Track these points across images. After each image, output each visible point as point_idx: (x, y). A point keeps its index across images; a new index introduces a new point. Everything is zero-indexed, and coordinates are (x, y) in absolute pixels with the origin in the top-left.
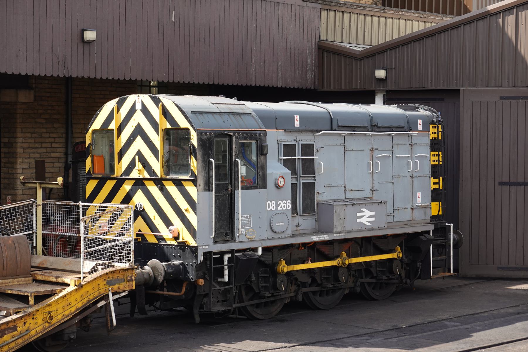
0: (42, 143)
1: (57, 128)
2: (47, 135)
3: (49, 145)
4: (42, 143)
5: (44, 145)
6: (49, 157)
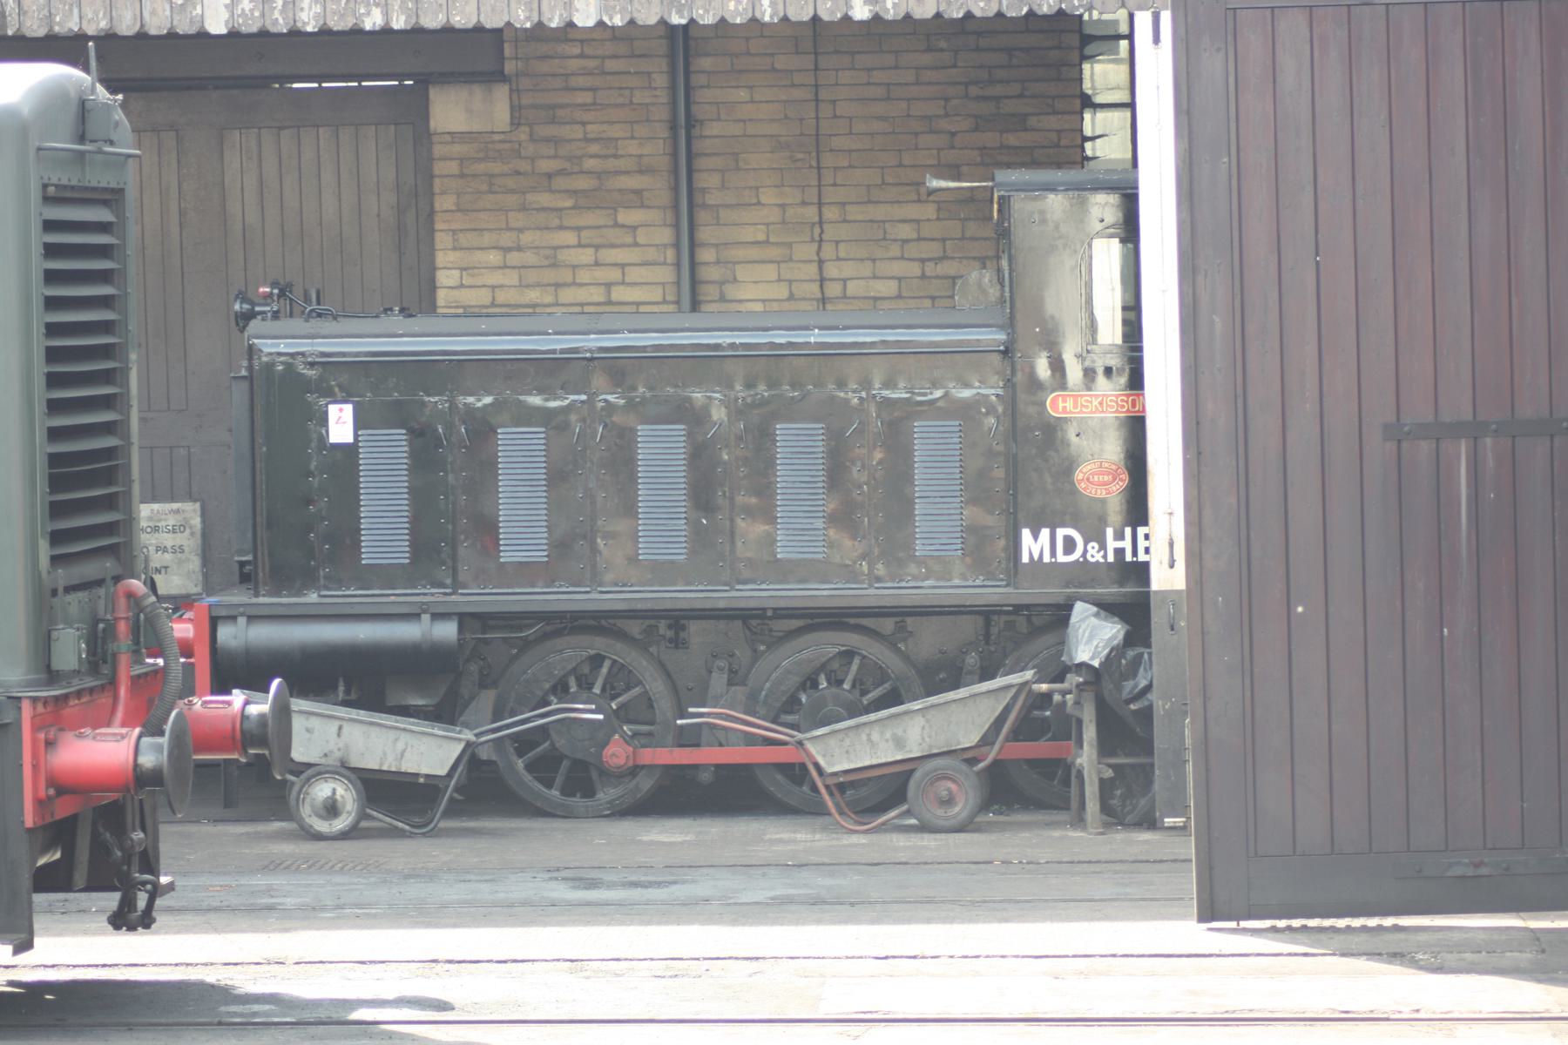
0: (557, 285)
1: (634, 228)
4: (557, 285)
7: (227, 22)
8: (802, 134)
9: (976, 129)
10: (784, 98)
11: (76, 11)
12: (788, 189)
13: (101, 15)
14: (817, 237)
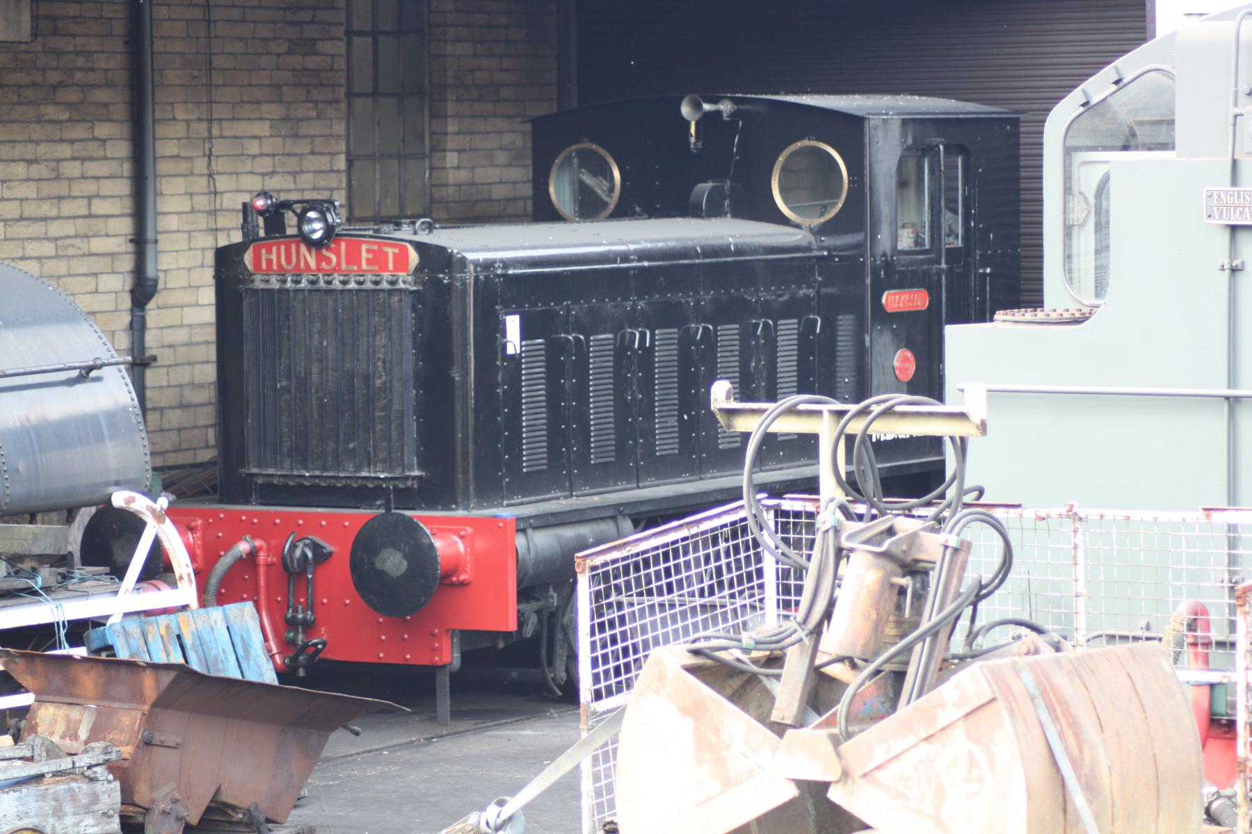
0: (60, 198)
2: (73, 169)
3: (79, 207)
4: (60, 198)
5: (68, 208)
6: (84, 255)
8: (197, 53)
9: (290, 52)
10: (188, 17)
12: (190, 105)
14: (207, 153)
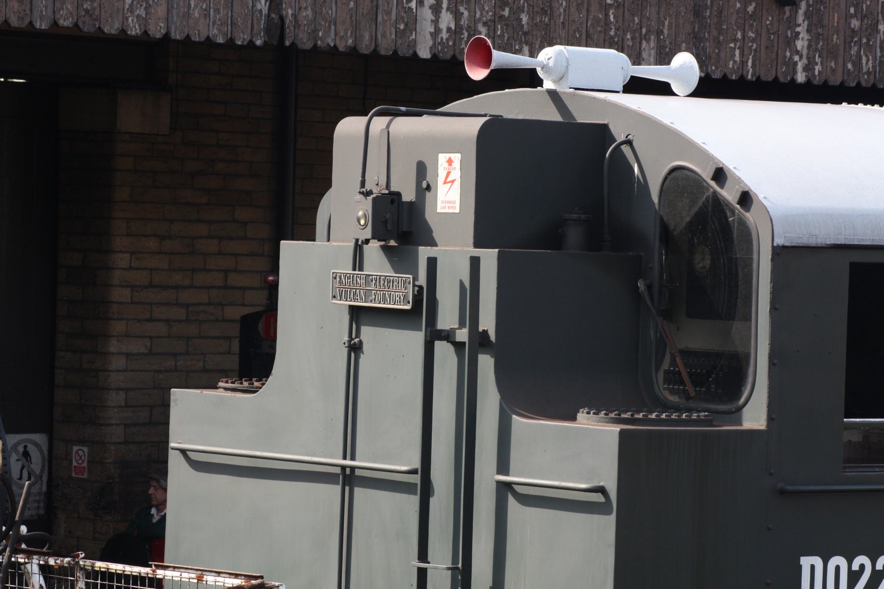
6: (217, 321)
7: (431, 48)
11: (333, 27)
13: (349, 34)
